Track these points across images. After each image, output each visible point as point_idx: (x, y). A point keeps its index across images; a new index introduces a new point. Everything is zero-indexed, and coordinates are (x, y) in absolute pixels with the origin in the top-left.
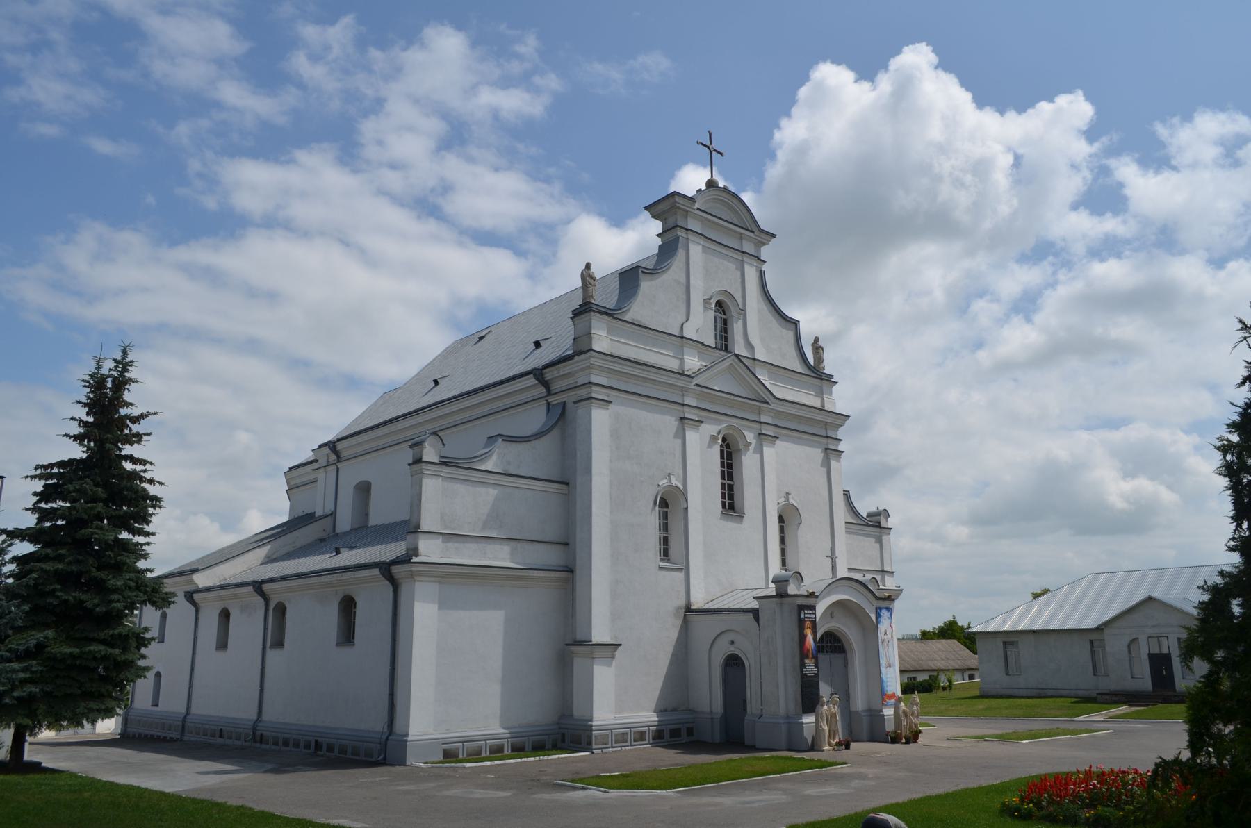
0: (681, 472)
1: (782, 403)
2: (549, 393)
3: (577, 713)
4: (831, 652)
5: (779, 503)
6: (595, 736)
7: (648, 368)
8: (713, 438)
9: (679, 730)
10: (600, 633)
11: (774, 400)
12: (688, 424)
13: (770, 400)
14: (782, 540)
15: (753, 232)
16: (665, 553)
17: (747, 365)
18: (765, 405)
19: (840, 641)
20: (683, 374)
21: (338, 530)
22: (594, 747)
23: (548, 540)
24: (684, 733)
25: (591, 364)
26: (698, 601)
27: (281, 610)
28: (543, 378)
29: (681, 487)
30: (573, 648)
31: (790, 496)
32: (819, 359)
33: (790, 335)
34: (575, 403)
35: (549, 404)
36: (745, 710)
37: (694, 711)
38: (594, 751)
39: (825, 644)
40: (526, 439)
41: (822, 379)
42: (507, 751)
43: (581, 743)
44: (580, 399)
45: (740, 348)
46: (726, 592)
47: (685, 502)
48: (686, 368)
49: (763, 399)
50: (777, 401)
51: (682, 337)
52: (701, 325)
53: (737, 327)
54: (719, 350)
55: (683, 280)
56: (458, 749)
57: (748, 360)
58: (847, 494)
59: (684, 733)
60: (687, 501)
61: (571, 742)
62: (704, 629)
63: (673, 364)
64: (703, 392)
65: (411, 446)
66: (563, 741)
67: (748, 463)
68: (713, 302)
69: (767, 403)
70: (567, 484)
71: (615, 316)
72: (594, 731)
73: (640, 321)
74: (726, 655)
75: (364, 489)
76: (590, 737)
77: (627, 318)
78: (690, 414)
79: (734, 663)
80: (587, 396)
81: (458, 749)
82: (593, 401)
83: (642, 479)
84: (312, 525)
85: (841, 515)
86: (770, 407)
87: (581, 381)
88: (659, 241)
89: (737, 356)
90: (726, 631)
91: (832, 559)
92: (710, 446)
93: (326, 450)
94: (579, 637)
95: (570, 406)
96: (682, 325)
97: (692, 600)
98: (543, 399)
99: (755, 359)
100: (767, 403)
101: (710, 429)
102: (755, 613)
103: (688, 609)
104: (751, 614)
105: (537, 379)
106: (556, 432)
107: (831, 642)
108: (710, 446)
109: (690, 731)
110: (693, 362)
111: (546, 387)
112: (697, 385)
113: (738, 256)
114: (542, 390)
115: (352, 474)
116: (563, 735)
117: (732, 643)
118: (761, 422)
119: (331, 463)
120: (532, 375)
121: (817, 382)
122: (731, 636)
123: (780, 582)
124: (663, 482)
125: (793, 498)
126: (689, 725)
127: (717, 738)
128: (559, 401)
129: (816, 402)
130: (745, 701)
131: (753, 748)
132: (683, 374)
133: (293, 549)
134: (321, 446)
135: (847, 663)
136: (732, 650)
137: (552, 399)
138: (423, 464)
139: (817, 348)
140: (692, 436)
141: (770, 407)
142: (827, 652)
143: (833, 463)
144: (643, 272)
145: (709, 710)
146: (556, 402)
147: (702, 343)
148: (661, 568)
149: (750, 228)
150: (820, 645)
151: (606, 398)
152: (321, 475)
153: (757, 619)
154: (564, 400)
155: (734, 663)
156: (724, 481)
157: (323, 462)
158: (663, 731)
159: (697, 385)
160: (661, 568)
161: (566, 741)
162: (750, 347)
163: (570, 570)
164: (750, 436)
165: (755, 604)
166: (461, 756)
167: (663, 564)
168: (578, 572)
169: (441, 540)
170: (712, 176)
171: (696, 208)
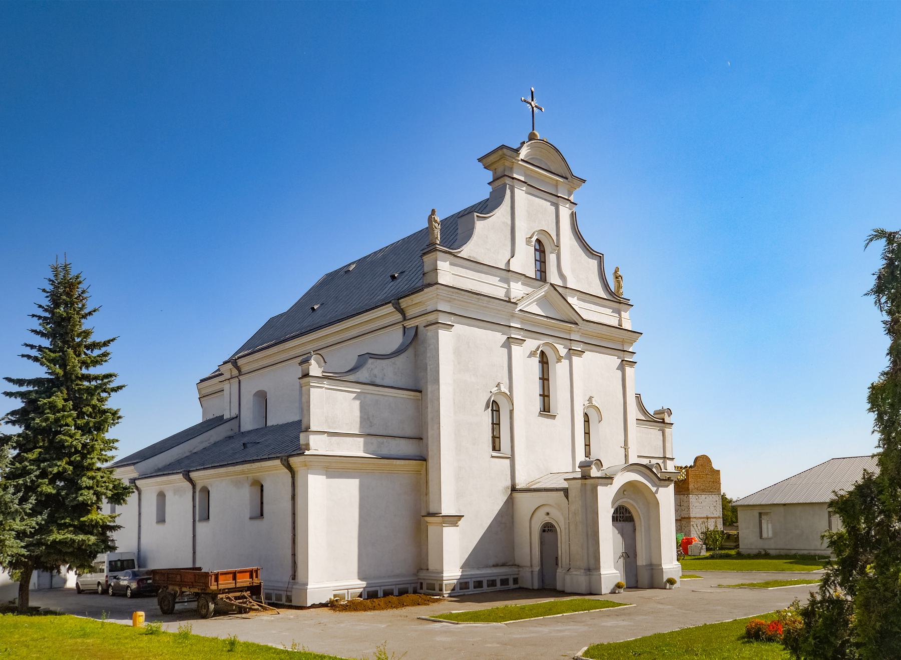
1: (588, 323)
2: (405, 319)
3: (432, 566)
5: (584, 405)
6: (445, 585)
7: (482, 297)
8: (533, 354)
9: (507, 580)
10: (447, 508)
12: (512, 342)
13: (578, 321)
14: (587, 433)
16: (496, 447)
17: (560, 292)
19: (630, 513)
20: (509, 302)
21: (243, 430)
22: (444, 592)
23: (407, 435)
24: (511, 582)
25: (438, 295)
26: (521, 483)
27: (206, 492)
28: (400, 307)
29: (509, 394)
30: (429, 519)
31: (593, 399)
32: (619, 287)
33: (594, 263)
34: (425, 327)
35: (404, 327)
36: (557, 564)
37: (518, 566)
38: (444, 595)
41: (620, 303)
43: (434, 590)
44: (429, 323)
45: (553, 277)
46: (542, 475)
47: (512, 406)
48: (512, 297)
49: (574, 320)
50: (585, 322)
51: (509, 271)
52: (524, 261)
53: (551, 259)
54: (538, 280)
55: (509, 222)
56: (345, 594)
58: (638, 397)
59: (511, 582)
60: (513, 405)
61: (427, 589)
62: (525, 504)
63: (501, 294)
65: (300, 364)
66: (421, 588)
67: (559, 371)
68: (534, 239)
69: (577, 324)
70: (420, 392)
72: (445, 580)
74: (543, 523)
75: (262, 397)
76: (441, 585)
79: (548, 529)
80: (434, 321)
81: (345, 594)
82: (440, 325)
83: (478, 387)
84: (222, 426)
85: (634, 413)
87: (429, 309)
88: (490, 189)
89: (551, 284)
90: (542, 505)
91: (625, 449)
93: (230, 366)
94: (432, 510)
95: (421, 329)
96: (509, 260)
97: (517, 481)
98: (400, 324)
99: (566, 288)
100: (577, 324)
101: (532, 344)
102: (566, 491)
103: (514, 489)
104: (563, 492)
105: (395, 308)
106: (410, 352)
107: (623, 514)
109: (516, 581)
111: (402, 314)
113: (554, 199)
114: (399, 317)
115: (251, 385)
116: (421, 584)
117: (548, 514)
118: (571, 340)
119: (233, 377)
120: (391, 304)
121: (616, 305)
122: (547, 509)
123: (585, 466)
124: (494, 390)
125: (595, 401)
126: (516, 576)
127: (536, 586)
128: (413, 326)
129: (614, 322)
130: (557, 558)
131: (563, 593)
132: (509, 302)
133: (208, 445)
134: (225, 363)
135: (635, 529)
136: (548, 519)
137: (407, 324)
138: (311, 378)
139: (617, 277)
140: (515, 348)
141: (580, 327)
142: (620, 521)
143: (628, 370)
144: (477, 216)
145: (529, 565)
146: (410, 326)
147: (524, 275)
148: (492, 457)
152: (226, 386)
153: (567, 497)
154: (417, 324)
155: (548, 529)
157: (227, 375)
158: (496, 580)
160: (492, 457)
161: (423, 588)
162: (562, 276)
163: (424, 459)
164: (563, 351)
165: (565, 485)
167: (495, 454)
168: (430, 461)
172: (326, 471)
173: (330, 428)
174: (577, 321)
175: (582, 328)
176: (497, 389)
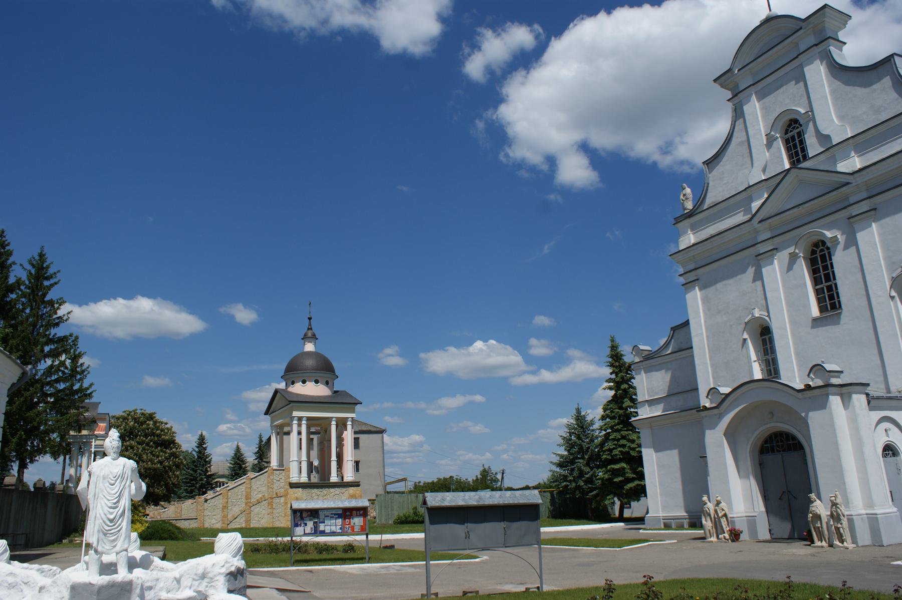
0: (764, 302)
1: (864, 172)
4: (783, 451)
8: (793, 257)
11: (851, 177)
15: (801, 28)
18: (844, 188)
19: (794, 438)
39: (775, 445)
40: (683, 325)
42: (686, 526)
49: (844, 182)
50: (856, 175)
55: (745, 138)
57: (822, 157)
64: (770, 222)
69: (848, 183)
71: (694, 214)
73: (714, 202)
77: (704, 209)
78: (762, 248)
83: (731, 323)
86: (854, 184)
92: (790, 267)
100: (848, 183)
108: (790, 267)
110: (755, 205)
112: (760, 222)
141: (854, 184)
142: (778, 451)
149: (798, 28)
150: (769, 445)
151: (695, 278)
156: (834, 282)
159: (760, 222)
166: (673, 527)
169: (647, 404)
170: (770, 10)
171: (736, 72)
172: (651, 429)
173: (651, 396)
174: (847, 181)
175: (858, 183)
176: (750, 316)
